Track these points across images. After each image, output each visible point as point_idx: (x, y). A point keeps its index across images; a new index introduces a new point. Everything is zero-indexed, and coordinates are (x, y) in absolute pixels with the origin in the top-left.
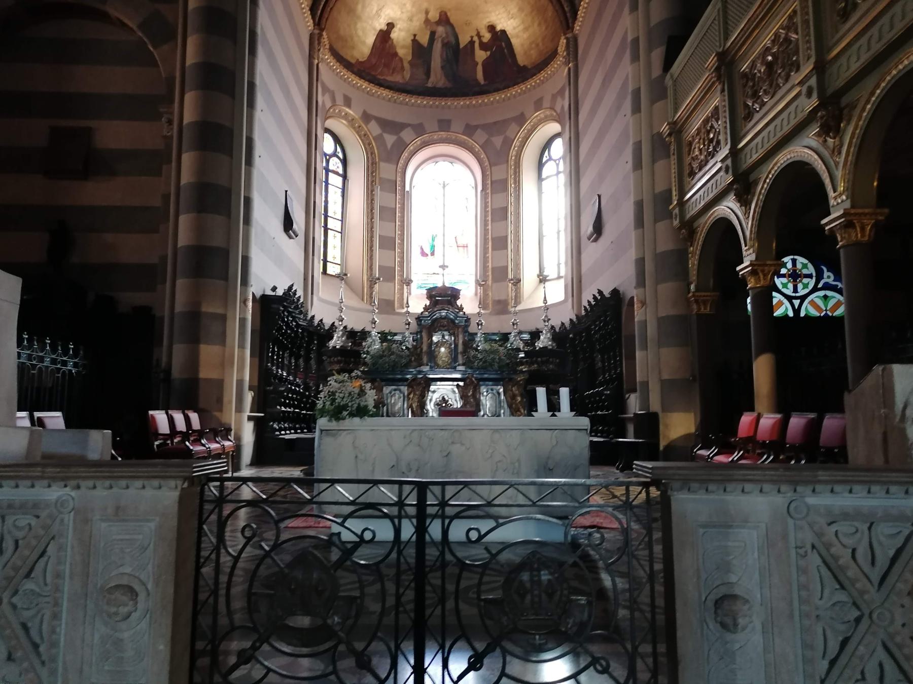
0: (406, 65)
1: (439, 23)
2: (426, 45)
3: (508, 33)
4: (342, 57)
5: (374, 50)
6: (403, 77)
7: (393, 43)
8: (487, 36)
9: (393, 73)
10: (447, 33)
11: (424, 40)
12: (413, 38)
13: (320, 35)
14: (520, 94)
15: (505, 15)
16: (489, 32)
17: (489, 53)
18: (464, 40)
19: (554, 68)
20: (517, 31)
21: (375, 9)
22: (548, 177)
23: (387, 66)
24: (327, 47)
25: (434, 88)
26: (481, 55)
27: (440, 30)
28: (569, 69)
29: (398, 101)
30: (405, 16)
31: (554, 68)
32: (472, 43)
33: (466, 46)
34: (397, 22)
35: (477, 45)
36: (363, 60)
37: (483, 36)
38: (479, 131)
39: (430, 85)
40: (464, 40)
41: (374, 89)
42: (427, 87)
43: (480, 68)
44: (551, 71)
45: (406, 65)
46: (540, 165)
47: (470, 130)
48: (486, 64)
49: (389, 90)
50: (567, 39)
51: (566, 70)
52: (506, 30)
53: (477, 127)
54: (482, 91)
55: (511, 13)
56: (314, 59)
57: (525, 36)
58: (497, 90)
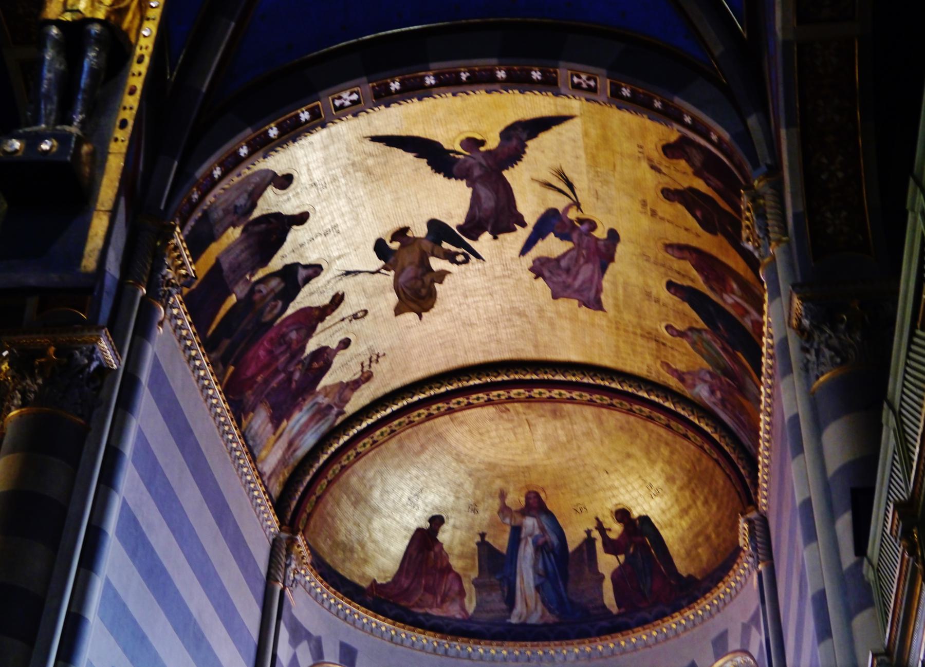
1: (525, 512)
2: (504, 551)
3: (653, 520)
4: (343, 579)
5: (406, 564)
6: (463, 608)
7: (442, 548)
8: (616, 529)
9: (443, 601)
10: (542, 529)
11: (501, 542)
12: (478, 539)
13: (292, 541)
14: (685, 629)
15: (643, 491)
16: (619, 521)
17: (622, 558)
18: (574, 537)
19: (741, 575)
20: (669, 515)
21: (407, 494)
23: (431, 590)
24: (308, 559)
25: (523, 625)
26: (607, 563)
27: (530, 523)
28: (760, 575)
29: (452, 652)
30: (463, 504)
31: (741, 575)
33: (579, 549)
34: (449, 514)
35: (599, 545)
36: (384, 582)
37: (610, 530)
39: (514, 620)
40: (574, 537)
41: (404, 633)
42: (511, 624)
44: (736, 582)
48: (617, 577)
49: (432, 633)
50: (749, 522)
51: (755, 576)
52: (649, 515)
55: (655, 485)
56: (277, 581)
57: (685, 523)
58: (643, 623)
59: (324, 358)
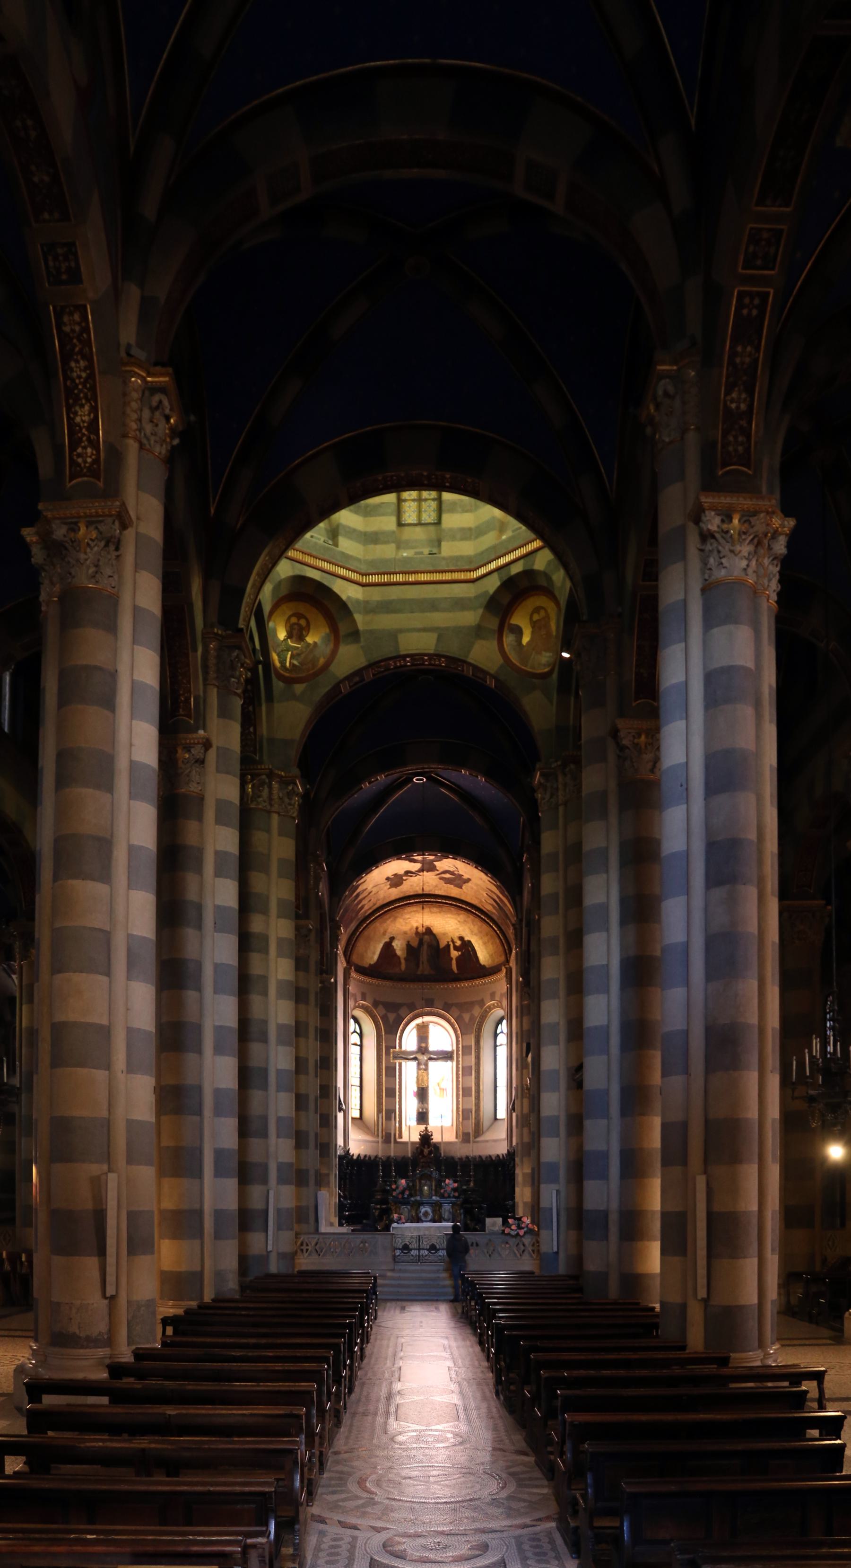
0: (403, 961)
1: (424, 934)
6: (401, 970)
8: (458, 943)
11: (415, 944)
17: (460, 953)
18: (443, 944)
22: (501, 1045)
27: (426, 938)
28: (507, 987)
32: (448, 946)
38: (454, 1008)
39: (419, 973)
40: (443, 944)
41: (380, 982)
43: (454, 962)
45: (403, 961)
46: (496, 1035)
47: (447, 1007)
50: (506, 968)
53: (452, 1005)
54: (457, 979)
58: (467, 979)
59: (362, 907)
